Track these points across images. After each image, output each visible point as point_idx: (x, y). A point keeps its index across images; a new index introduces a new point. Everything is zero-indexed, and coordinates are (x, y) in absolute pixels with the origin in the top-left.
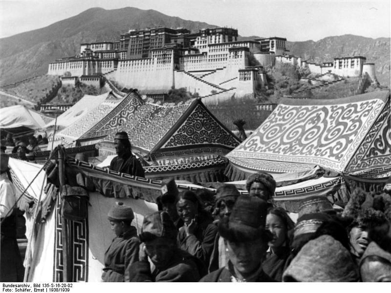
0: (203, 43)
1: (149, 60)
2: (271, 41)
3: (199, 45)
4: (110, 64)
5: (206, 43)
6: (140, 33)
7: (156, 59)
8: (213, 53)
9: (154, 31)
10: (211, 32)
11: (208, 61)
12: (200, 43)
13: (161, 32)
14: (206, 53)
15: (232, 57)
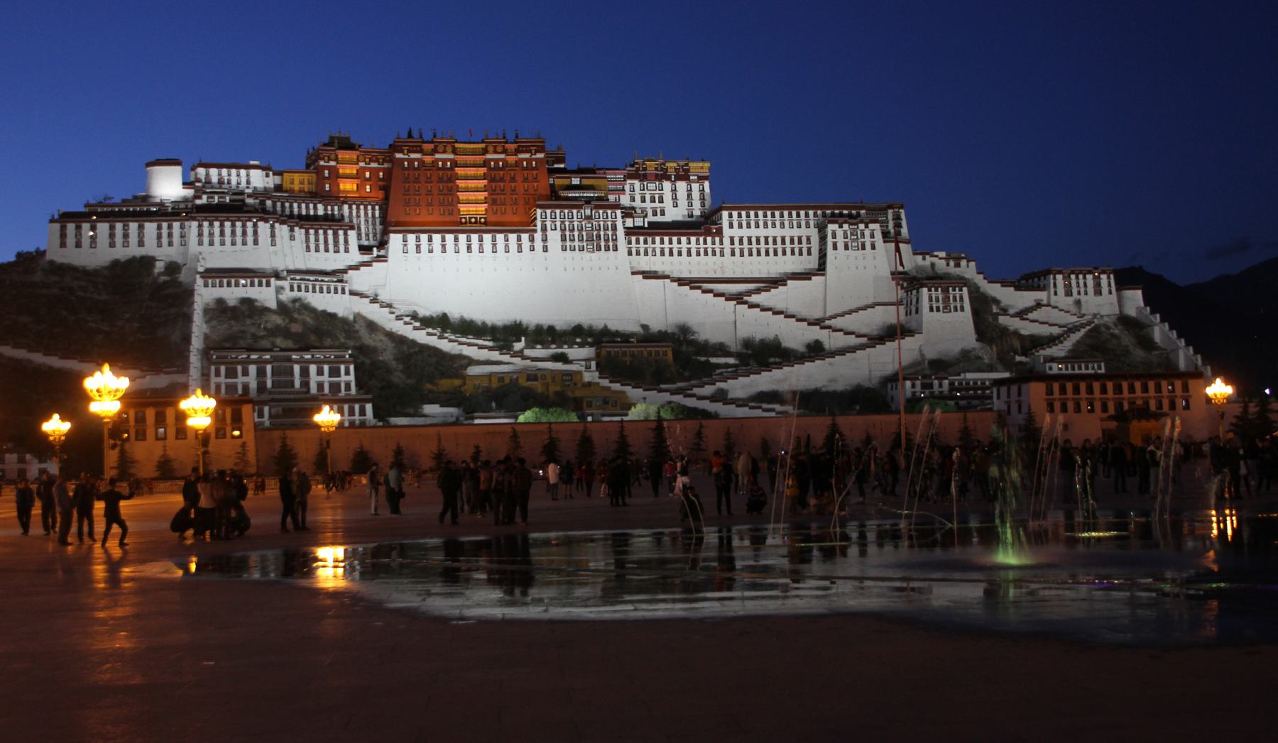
0: (653, 200)
1: (525, 237)
2: (890, 211)
3: (638, 203)
4: (341, 238)
5: (661, 201)
6: (441, 148)
7: (554, 237)
8: (745, 232)
9: (499, 149)
10: (671, 172)
11: (727, 251)
12: (638, 198)
13: (530, 151)
14: (720, 233)
15: (841, 246)
